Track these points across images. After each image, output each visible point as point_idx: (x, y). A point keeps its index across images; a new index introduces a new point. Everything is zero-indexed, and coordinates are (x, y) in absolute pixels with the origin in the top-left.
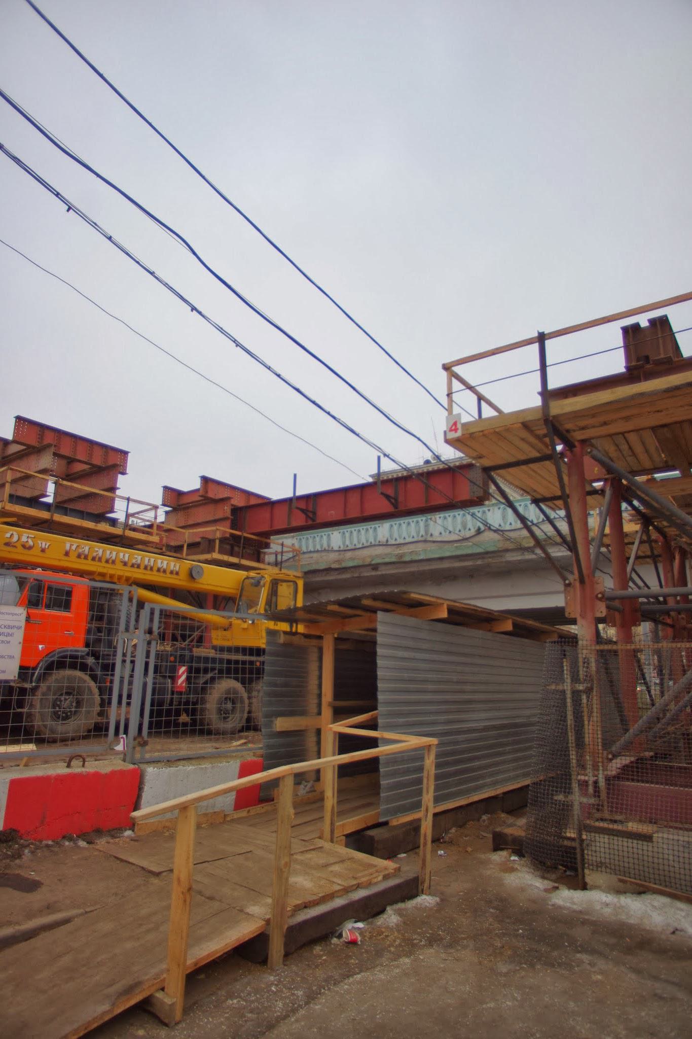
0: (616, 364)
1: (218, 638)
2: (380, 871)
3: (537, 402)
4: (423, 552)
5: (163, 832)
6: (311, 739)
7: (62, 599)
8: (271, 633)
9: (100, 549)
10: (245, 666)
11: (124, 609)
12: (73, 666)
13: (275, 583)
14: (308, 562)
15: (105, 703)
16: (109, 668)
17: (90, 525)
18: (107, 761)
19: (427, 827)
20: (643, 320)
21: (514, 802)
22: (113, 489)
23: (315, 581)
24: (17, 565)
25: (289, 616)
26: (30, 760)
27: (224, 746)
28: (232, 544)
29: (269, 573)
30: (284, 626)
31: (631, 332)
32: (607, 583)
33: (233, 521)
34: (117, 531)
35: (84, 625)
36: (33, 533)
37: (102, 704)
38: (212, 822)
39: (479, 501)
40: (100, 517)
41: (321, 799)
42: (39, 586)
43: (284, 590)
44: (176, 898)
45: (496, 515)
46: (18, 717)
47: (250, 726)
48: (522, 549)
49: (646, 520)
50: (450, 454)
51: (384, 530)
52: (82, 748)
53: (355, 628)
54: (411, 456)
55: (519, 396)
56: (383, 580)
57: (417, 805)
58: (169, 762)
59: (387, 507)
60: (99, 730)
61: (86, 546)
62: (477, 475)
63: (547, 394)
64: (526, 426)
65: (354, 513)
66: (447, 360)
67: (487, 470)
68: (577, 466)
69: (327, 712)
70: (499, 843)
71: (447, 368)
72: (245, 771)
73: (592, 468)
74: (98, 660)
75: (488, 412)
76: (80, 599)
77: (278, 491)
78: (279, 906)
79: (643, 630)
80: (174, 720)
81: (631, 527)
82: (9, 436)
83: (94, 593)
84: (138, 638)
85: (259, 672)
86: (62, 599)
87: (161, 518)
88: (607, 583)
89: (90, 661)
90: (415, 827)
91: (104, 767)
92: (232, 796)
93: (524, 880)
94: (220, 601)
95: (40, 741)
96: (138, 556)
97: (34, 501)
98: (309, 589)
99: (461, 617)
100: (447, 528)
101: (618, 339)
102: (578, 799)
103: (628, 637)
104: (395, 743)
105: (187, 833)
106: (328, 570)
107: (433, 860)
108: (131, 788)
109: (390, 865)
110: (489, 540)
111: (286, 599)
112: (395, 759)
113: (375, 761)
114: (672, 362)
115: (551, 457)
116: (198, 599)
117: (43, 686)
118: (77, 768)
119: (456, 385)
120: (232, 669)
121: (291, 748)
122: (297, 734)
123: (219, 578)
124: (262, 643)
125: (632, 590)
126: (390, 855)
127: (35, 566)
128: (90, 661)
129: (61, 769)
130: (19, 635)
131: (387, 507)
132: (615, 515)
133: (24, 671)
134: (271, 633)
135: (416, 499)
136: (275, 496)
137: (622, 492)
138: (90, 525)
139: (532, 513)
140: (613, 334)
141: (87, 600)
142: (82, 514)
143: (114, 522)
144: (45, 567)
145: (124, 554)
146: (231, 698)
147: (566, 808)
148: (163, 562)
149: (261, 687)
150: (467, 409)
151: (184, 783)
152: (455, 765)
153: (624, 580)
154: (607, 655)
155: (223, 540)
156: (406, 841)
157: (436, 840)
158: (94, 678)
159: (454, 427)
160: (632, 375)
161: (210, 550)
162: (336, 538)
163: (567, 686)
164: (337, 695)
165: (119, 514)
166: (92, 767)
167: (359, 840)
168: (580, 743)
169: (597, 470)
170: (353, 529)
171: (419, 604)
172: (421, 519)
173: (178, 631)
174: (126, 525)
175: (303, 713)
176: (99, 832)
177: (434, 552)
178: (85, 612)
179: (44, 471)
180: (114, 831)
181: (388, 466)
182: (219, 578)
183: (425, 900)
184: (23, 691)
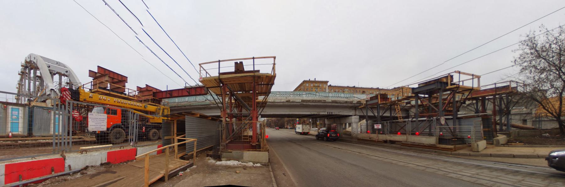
0: (233, 69)
1: (151, 121)
2: (186, 163)
3: (218, 75)
4: (195, 104)
5: (142, 160)
6: (172, 140)
7: (115, 112)
8: (163, 120)
9: (123, 101)
10: (158, 126)
11: (130, 115)
12: (119, 127)
13: (164, 109)
14: (171, 105)
15: (127, 135)
16: (128, 128)
17: (120, 95)
18: (129, 147)
19: (195, 154)
20: (238, 62)
21: (210, 149)
22: (125, 86)
23: (172, 109)
24: (103, 104)
25: (167, 116)
26: (111, 148)
27: (154, 143)
28: (153, 101)
29: (162, 107)
30: (166, 118)
31: (236, 63)
32: (228, 111)
33: (153, 95)
34: (127, 96)
35: (121, 118)
36: (106, 96)
37: (126, 135)
38: (152, 157)
39: (206, 94)
40: (122, 93)
41: (174, 151)
42: (109, 109)
43: (165, 111)
44: (146, 171)
45: (209, 97)
46: (107, 139)
47: (159, 138)
48: (214, 104)
49: (235, 100)
50: (200, 84)
51: (187, 99)
52: (123, 145)
53: (181, 118)
54: (193, 84)
55: (215, 74)
56: (186, 109)
57: (193, 151)
58: (142, 146)
59: (187, 94)
60: (126, 141)
61: (119, 100)
62: (206, 89)
63: (220, 74)
64: (215, 79)
65: (180, 95)
66: (200, 63)
67: (207, 88)
68: (224, 89)
69: (175, 135)
70: (208, 156)
71: (200, 65)
72: (159, 147)
73: (227, 90)
74: (125, 125)
75: (208, 76)
76: (119, 112)
77: (163, 89)
78: (167, 171)
79: (234, 119)
80: (143, 138)
81: (233, 101)
82: (97, 71)
83: (122, 111)
84: (134, 121)
85: (161, 128)
86: (115, 112)
87: (137, 94)
88: (228, 111)
89: (123, 126)
90: (193, 155)
91: (131, 148)
92: (156, 152)
93: (212, 161)
94: (152, 113)
95: (113, 144)
96: (132, 103)
97: (105, 89)
98: (171, 111)
99: (202, 117)
100: (200, 99)
101: (234, 65)
102: (221, 147)
103: (231, 120)
104: (189, 140)
105: (147, 159)
106: (175, 107)
107: (196, 159)
108: (135, 152)
109: (188, 161)
110: (208, 102)
111: (166, 113)
112: (189, 143)
113: (185, 143)
114: (243, 71)
115: (220, 86)
116: (147, 112)
117: (112, 132)
118: (122, 149)
119: (202, 69)
120: (155, 127)
121: (168, 142)
122: (170, 139)
123: (151, 108)
124: (161, 122)
125: (232, 112)
126: (188, 160)
127: (107, 104)
128: (123, 126)
129: (119, 149)
130: (106, 121)
131: (187, 94)
132: (230, 99)
133: (108, 129)
134: (163, 120)
135: (194, 93)
136: (163, 90)
137: (232, 95)
138: (120, 95)
139: (216, 97)
140: (233, 64)
141: (121, 112)
142: (117, 92)
143: (125, 94)
144: (110, 105)
145: (129, 102)
146: (155, 133)
147: (219, 149)
148: (138, 104)
149: (161, 131)
150: (204, 75)
151: (145, 151)
152: (200, 143)
153: (231, 111)
154: (227, 123)
155: (151, 100)
156: (191, 157)
157: (196, 156)
158: (124, 130)
159: (201, 78)
160: (236, 72)
161: (148, 102)
162: (177, 100)
163: (220, 129)
164: (177, 132)
165: (127, 92)
166: (125, 148)
167: (182, 158)
168: (222, 139)
169: (228, 90)
170: (180, 98)
171: (194, 114)
172: (194, 97)
173: (142, 119)
174: (129, 95)
175: (170, 135)
176: (128, 161)
177: (197, 104)
178: (121, 116)
179: (107, 81)
180: (132, 160)
181: (187, 85)
182: (151, 108)
183: (194, 166)
184: (108, 133)
